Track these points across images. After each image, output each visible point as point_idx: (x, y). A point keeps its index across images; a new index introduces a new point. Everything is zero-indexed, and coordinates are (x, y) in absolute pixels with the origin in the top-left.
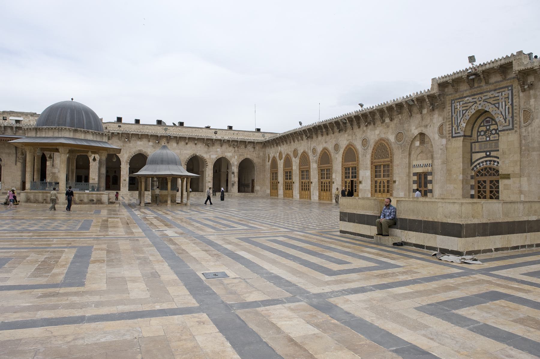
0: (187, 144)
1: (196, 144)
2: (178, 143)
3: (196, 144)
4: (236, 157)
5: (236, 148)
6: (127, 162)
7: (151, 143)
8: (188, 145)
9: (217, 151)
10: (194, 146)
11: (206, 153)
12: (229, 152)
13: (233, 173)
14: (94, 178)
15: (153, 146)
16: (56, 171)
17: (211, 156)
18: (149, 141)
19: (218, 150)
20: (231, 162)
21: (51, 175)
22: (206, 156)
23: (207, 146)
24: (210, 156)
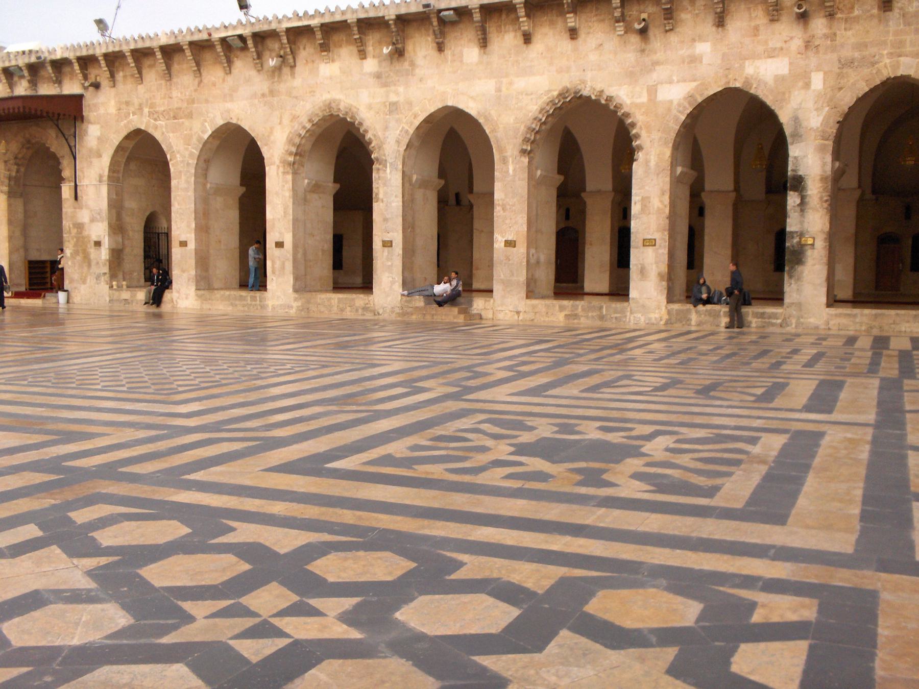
0: (527, 39)
1: (573, 33)
2: (484, 43)
3: (573, 33)
4: (818, 81)
5: (819, 25)
6: (284, 162)
7: (371, 65)
8: (538, 46)
9: (694, 60)
10: (566, 45)
11: (631, 76)
12: (771, 54)
13: (798, 183)
14: (183, 239)
15: (378, 76)
16: (84, 216)
17: (656, 84)
18: (363, 54)
19: (703, 48)
20: (784, 117)
21: (74, 231)
22: (627, 96)
23: (635, 39)
24: (652, 91)
